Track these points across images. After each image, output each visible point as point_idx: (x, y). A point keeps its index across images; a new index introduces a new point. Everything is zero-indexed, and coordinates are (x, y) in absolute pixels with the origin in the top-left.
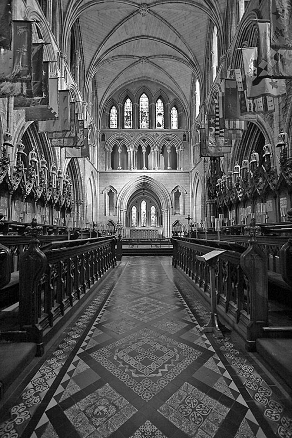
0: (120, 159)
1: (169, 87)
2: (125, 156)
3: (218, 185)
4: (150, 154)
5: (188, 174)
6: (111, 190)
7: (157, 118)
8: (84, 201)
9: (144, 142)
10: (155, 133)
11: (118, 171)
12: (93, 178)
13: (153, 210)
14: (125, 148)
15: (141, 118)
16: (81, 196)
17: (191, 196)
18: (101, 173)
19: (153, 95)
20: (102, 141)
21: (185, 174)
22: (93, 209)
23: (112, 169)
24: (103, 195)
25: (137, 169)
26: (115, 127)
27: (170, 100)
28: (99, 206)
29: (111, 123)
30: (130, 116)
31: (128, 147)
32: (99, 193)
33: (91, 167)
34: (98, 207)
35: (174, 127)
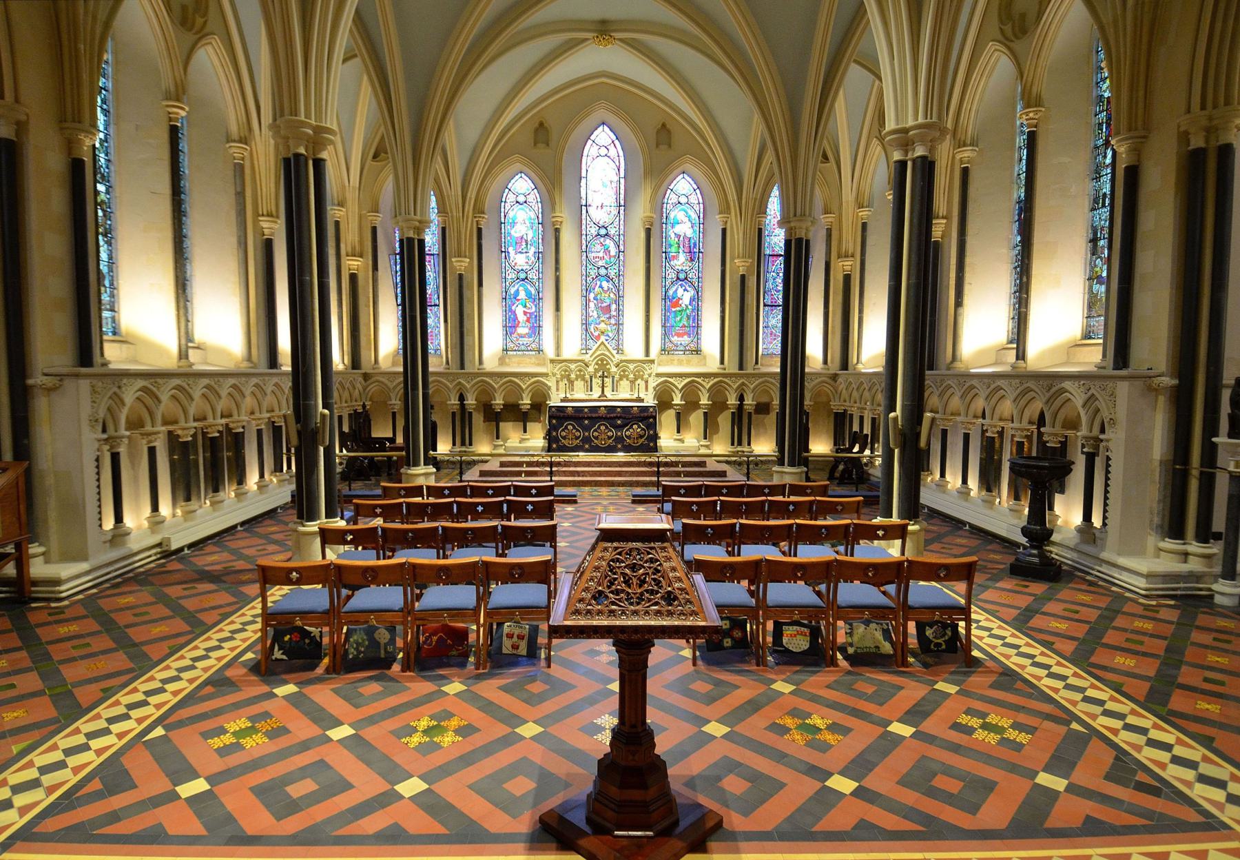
13: (677, 214)
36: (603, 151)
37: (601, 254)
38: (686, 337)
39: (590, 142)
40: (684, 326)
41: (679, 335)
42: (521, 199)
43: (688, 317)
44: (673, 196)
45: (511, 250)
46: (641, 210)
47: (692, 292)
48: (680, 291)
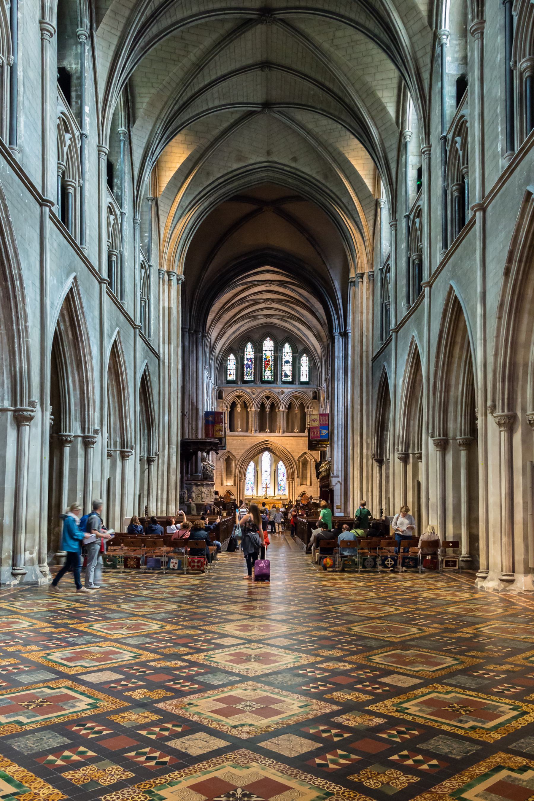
1: (298, 335)
2: (245, 413)
6: (229, 457)
7: (283, 367)
9: (268, 400)
10: (280, 390)
11: (237, 434)
14: (245, 406)
15: (265, 367)
19: (279, 344)
20: (219, 399)
23: (230, 431)
26: (232, 377)
27: (299, 351)
29: (228, 373)
30: (252, 365)
31: (249, 406)
35: (304, 378)
46: (273, 468)
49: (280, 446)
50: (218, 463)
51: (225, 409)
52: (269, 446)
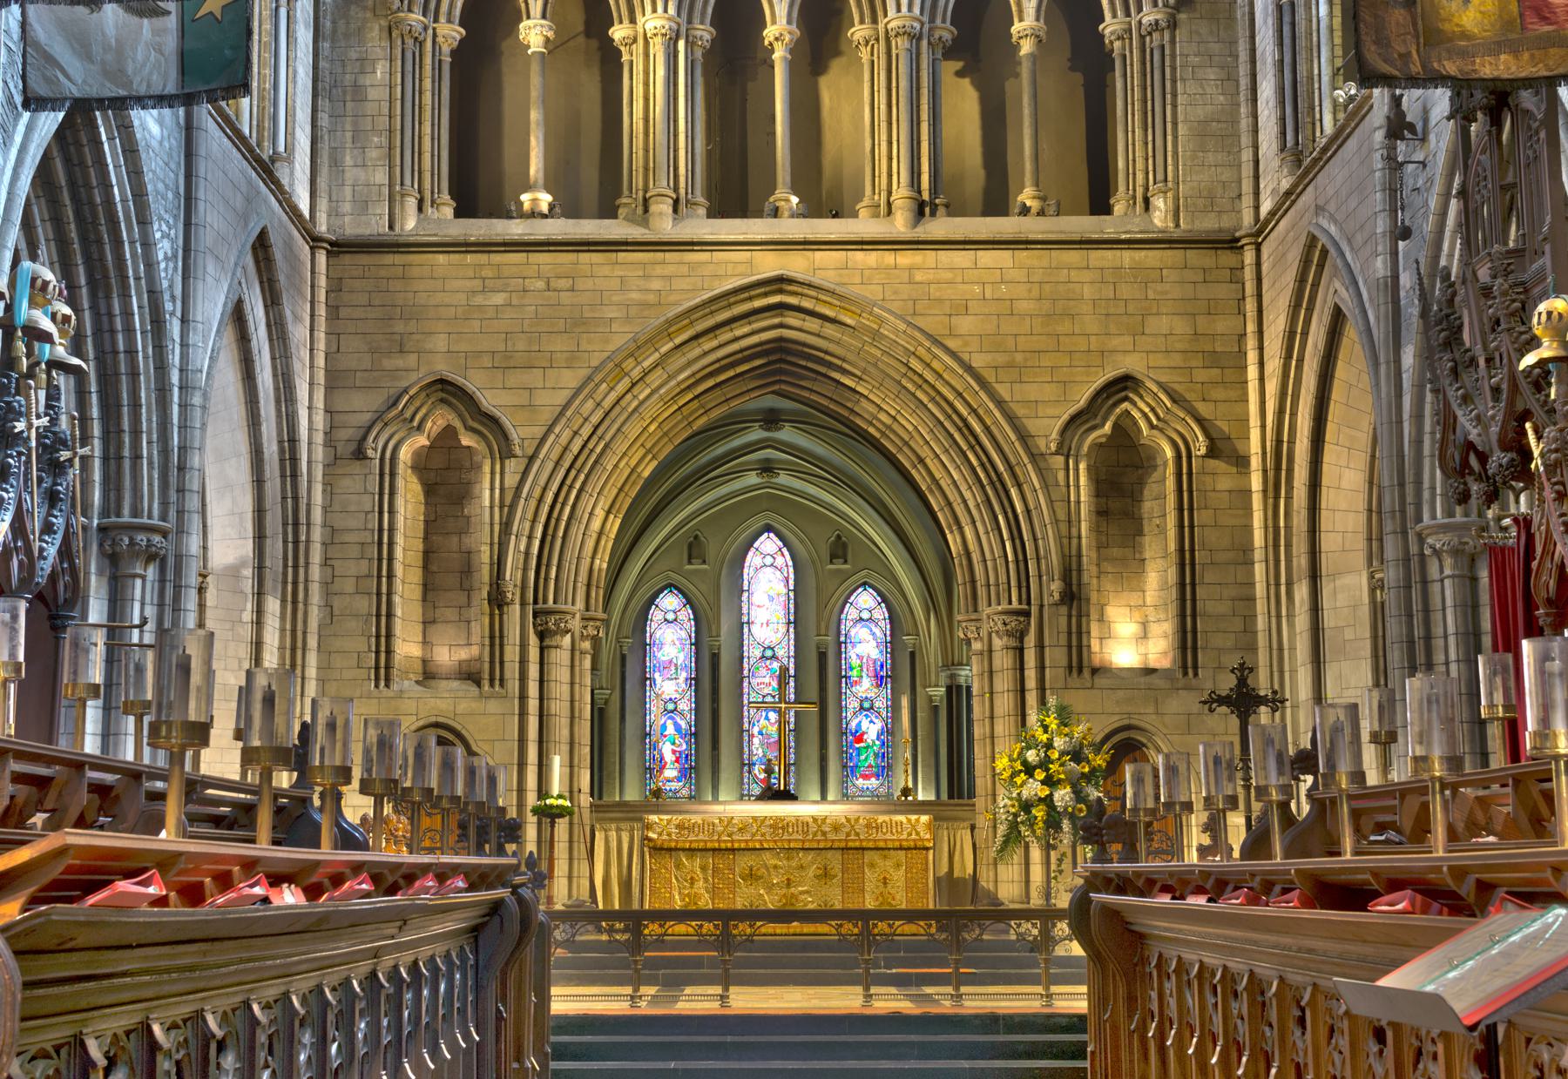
0: (535, 115)
2: (590, 85)
3: (1542, 363)
4: (836, 66)
5: (1227, 258)
8: (181, 530)
11: (515, 229)
12: (272, 300)
13: (860, 633)
16: (149, 477)
17: (1256, 482)
18: (347, 259)
21: (1194, 256)
22: (259, 611)
23: (459, 214)
24: (359, 485)
25: (711, 214)
28: (326, 585)
32: (319, 453)
33: (251, 199)
34: (316, 597)
36: (769, 560)
37: (767, 680)
38: (873, 779)
39: (753, 550)
40: (870, 766)
41: (866, 777)
42: (671, 616)
43: (876, 755)
44: (853, 610)
45: (657, 675)
47: (879, 725)
48: (865, 725)
49: (893, 328)
50: (346, 483)
51: (416, 18)
52: (799, 329)
